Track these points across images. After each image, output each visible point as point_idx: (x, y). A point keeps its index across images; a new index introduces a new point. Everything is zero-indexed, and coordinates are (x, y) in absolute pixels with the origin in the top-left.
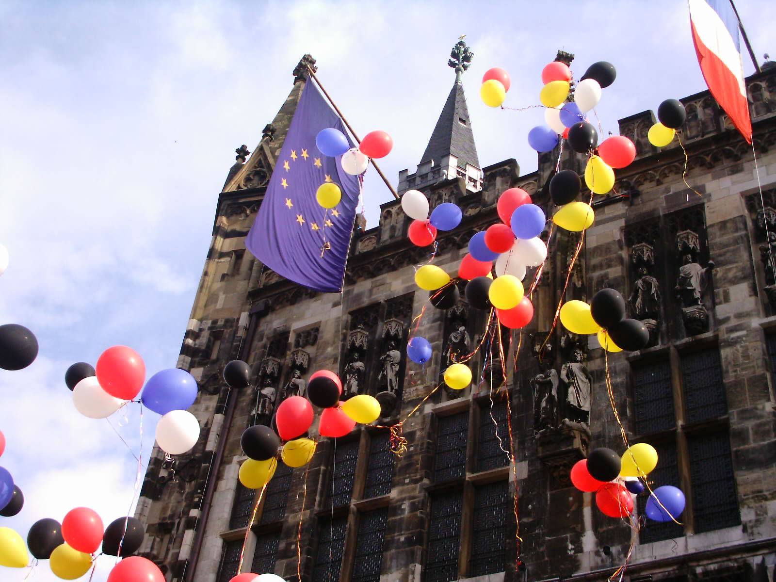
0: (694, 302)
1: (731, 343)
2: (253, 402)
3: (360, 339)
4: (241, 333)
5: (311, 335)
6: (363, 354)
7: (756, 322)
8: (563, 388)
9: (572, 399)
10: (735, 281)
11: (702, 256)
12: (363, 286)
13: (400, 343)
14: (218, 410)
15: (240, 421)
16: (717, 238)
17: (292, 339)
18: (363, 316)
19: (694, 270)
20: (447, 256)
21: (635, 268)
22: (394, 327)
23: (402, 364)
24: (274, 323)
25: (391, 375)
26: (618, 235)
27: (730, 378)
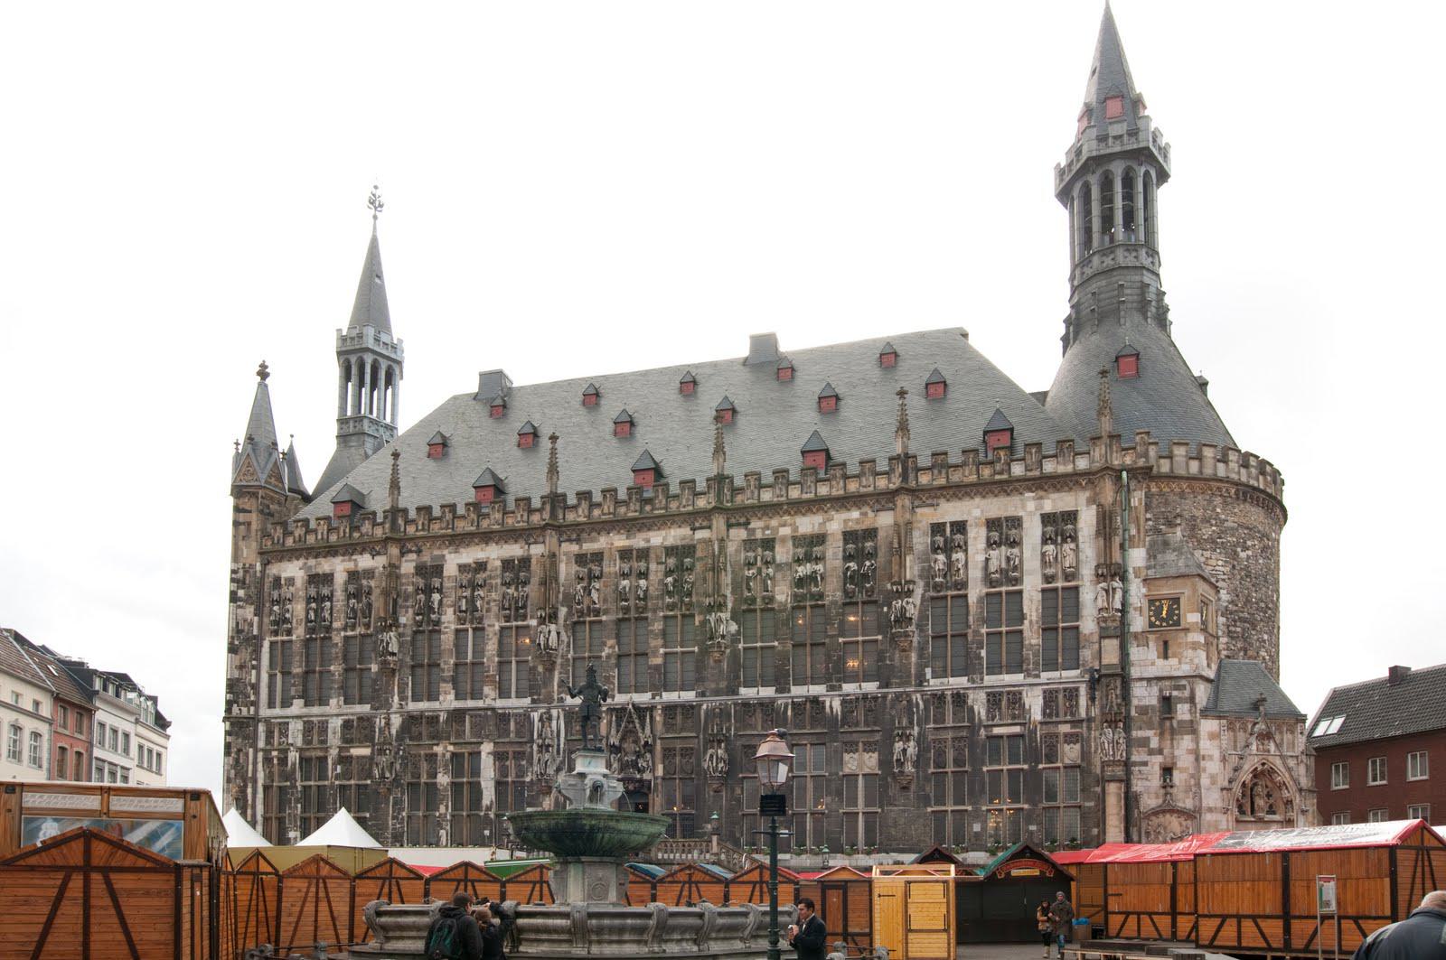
0: (434, 613)
1: (445, 633)
2: (271, 614)
3: (313, 592)
4: (258, 574)
5: (291, 581)
6: (315, 600)
7: (453, 627)
8: (388, 644)
9: (390, 649)
10: (450, 606)
11: (440, 591)
12: (312, 562)
13: (330, 598)
14: (255, 615)
15: (266, 620)
16: (447, 584)
17: (283, 582)
18: (314, 579)
19: (436, 597)
20: (346, 558)
21: (417, 590)
22: (325, 591)
23: (331, 609)
24: (274, 570)
25: (327, 616)
26: (412, 571)
27: (442, 648)
